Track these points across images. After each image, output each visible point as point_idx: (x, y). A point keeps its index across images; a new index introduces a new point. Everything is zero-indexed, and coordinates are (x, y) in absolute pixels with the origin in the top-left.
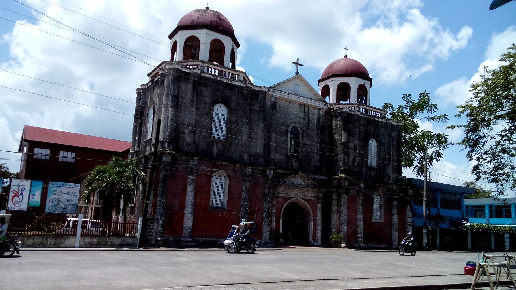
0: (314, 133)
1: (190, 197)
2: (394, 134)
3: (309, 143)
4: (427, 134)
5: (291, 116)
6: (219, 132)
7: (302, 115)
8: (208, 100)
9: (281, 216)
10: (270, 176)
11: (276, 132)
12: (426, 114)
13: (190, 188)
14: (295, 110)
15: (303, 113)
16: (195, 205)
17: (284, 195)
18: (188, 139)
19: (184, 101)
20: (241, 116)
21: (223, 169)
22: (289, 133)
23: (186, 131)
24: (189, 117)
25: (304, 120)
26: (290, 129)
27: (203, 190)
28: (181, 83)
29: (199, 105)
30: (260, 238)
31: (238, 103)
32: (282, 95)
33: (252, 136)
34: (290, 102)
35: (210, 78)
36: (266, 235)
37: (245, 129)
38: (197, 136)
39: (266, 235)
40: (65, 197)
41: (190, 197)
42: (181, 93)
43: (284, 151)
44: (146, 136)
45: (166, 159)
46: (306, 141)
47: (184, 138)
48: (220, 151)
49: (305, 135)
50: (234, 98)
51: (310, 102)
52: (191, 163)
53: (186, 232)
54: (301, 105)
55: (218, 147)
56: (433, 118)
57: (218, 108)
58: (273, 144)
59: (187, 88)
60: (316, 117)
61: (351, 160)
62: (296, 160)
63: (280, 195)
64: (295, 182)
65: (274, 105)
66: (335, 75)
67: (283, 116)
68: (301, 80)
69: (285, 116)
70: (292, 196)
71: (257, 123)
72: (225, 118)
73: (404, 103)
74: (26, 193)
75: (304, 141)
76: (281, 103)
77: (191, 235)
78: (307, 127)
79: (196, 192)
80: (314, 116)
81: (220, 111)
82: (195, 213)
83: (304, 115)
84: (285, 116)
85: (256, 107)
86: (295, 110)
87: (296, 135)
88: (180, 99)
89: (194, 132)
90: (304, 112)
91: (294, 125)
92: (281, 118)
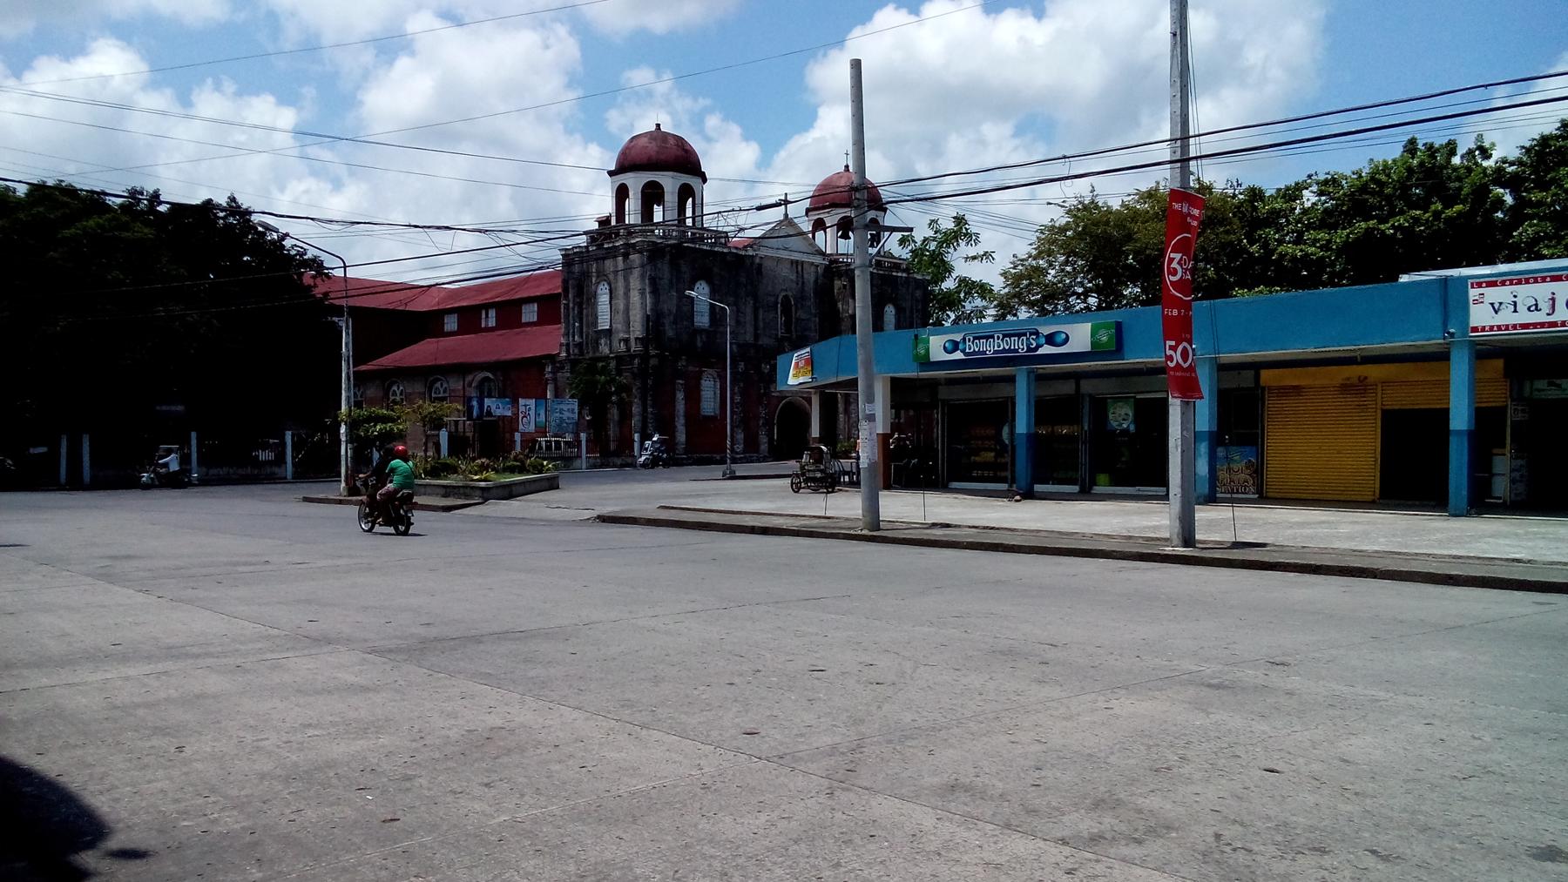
0: (811, 302)
1: (680, 406)
2: (918, 293)
3: (804, 316)
4: (968, 286)
7: (793, 277)
8: (687, 276)
12: (964, 249)
13: (680, 396)
14: (786, 272)
16: (687, 416)
18: (670, 333)
24: (670, 305)
27: (694, 397)
30: (757, 451)
32: (770, 253)
34: (779, 260)
36: (764, 447)
39: (764, 447)
40: (566, 415)
41: (680, 406)
44: (595, 323)
45: (653, 362)
46: (802, 314)
50: (716, 270)
51: (805, 258)
53: (681, 447)
54: (792, 262)
56: (974, 258)
60: (812, 279)
66: (834, 205)
73: (931, 233)
74: (532, 413)
76: (767, 263)
77: (686, 451)
78: (801, 297)
79: (686, 398)
80: (810, 277)
81: (700, 293)
82: (687, 425)
85: (743, 280)
86: (786, 272)
87: (787, 310)
89: (675, 322)
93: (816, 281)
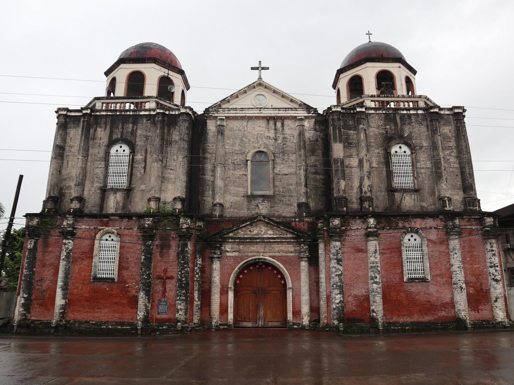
5: (252, 140)
6: (118, 178)
8: (105, 141)
9: (231, 285)
10: (185, 226)
11: (224, 165)
15: (273, 131)
17: (236, 254)
19: (73, 150)
20: (151, 152)
21: (113, 226)
22: (249, 162)
23: (72, 184)
25: (276, 140)
26: (249, 157)
28: (68, 130)
29: (91, 151)
31: (146, 137)
33: (167, 175)
35: (107, 115)
37: (154, 167)
38: (86, 189)
42: (68, 140)
43: (241, 190)
47: (70, 193)
48: (117, 203)
49: (278, 160)
52: (65, 223)
55: (115, 197)
57: (119, 149)
58: (219, 183)
59: (75, 134)
60: (296, 133)
61: (356, 184)
62: (263, 201)
63: (228, 254)
64: (256, 232)
65: (221, 130)
67: (238, 142)
68: (266, 87)
69: (242, 140)
70: (250, 254)
71: (175, 157)
72: (127, 159)
75: (276, 171)
83: (276, 133)
84: (242, 140)
88: (67, 149)
90: (275, 129)
91: (257, 150)
92: (234, 144)
93: (301, 134)
